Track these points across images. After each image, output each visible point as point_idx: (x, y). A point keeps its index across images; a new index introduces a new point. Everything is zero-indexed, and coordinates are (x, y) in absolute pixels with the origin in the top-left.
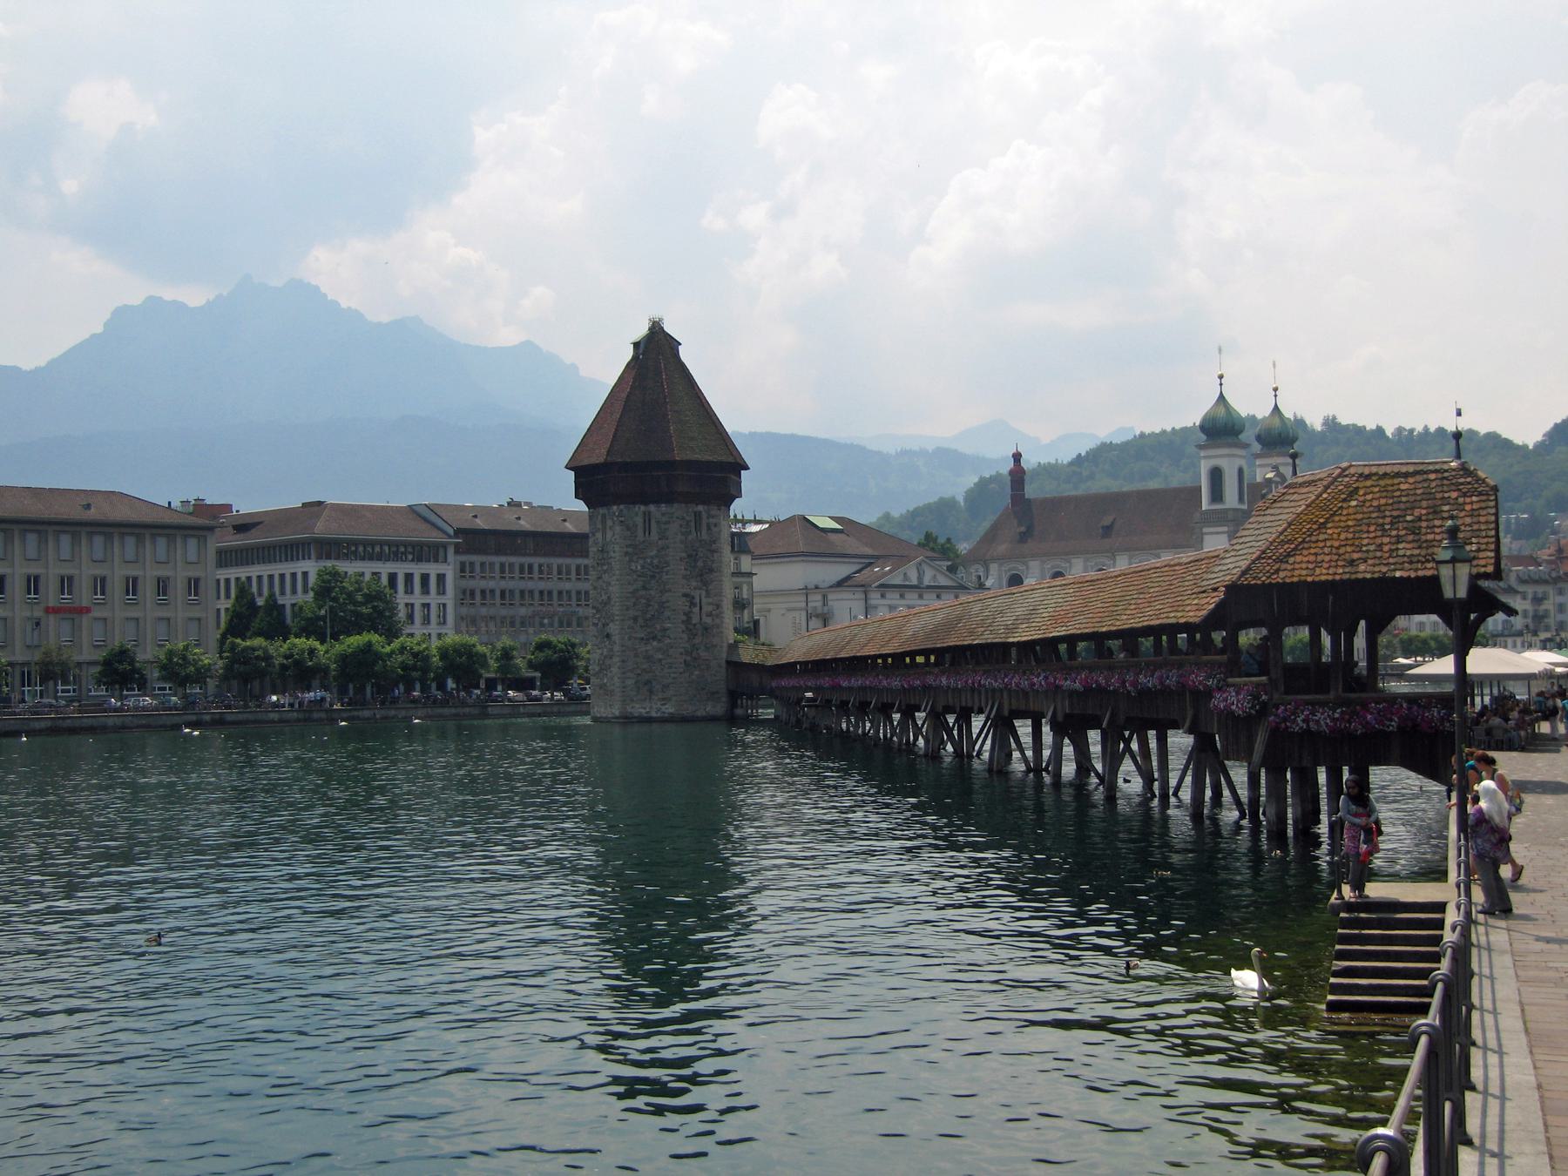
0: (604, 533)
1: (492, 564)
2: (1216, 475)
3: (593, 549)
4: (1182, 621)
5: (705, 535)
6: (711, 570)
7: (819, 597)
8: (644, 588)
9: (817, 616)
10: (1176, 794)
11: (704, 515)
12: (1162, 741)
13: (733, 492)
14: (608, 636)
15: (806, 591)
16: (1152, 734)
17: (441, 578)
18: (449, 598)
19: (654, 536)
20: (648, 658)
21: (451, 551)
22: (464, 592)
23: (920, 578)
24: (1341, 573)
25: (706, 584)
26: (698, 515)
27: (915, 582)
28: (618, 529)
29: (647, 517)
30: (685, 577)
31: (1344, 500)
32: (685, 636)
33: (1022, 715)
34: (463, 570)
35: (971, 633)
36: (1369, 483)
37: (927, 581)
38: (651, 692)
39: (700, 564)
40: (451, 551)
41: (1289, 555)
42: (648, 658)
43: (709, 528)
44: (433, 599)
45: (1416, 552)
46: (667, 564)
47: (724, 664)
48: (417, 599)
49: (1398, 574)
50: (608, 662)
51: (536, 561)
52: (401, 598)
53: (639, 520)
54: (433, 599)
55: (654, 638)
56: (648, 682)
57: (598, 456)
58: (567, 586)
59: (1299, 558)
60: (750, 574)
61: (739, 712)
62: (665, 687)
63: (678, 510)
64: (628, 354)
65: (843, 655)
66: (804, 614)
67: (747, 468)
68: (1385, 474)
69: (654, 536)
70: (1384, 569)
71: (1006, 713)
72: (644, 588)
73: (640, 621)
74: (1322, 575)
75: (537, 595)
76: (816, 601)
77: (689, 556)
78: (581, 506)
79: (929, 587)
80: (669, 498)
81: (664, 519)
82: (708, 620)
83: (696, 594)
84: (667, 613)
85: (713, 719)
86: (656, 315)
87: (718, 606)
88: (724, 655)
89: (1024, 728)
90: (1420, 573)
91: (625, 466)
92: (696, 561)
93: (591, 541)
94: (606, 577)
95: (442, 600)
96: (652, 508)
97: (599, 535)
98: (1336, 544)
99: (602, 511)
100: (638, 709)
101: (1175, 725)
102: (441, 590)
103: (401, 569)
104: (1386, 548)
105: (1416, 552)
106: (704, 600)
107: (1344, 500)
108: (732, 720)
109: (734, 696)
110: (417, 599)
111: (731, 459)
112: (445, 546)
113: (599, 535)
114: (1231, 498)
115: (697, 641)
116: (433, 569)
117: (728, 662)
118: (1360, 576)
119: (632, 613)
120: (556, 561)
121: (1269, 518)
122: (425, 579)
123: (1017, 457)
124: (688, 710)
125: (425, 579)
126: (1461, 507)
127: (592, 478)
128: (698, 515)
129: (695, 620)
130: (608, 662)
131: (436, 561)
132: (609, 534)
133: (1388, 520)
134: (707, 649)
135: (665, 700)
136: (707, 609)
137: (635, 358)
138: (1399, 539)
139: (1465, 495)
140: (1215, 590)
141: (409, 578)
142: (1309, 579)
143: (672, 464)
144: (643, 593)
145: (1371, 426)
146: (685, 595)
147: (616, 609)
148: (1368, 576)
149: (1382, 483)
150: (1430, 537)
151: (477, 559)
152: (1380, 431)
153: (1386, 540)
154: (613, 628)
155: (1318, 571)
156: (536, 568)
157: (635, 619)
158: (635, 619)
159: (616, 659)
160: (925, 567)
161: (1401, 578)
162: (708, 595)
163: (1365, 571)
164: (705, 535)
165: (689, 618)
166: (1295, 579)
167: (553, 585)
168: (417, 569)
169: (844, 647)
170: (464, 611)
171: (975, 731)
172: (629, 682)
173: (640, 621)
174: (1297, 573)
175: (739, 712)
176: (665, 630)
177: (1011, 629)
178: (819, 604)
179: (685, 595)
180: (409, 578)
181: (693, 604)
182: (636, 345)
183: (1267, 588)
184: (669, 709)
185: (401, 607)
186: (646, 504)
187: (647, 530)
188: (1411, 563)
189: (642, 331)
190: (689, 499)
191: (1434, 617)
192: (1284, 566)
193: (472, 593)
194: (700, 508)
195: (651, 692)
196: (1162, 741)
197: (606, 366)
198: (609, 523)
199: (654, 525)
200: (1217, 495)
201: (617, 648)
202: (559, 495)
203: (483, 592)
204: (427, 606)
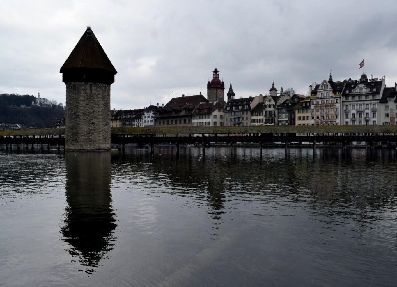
14: (93, 123)
20: (105, 131)
38: (105, 141)
42: (105, 131)
53: (104, 89)
55: (106, 125)
56: (105, 138)
69: (107, 94)
72: (105, 110)
73: (104, 119)
94: (92, 105)
99: (89, 83)
113: (88, 91)
127: (71, 72)
132: (94, 92)
144: (104, 111)
154: (94, 121)
157: (103, 119)
172: (102, 138)
173: (104, 119)
186: (105, 84)
195: (105, 141)
198: (94, 88)
201: (97, 127)
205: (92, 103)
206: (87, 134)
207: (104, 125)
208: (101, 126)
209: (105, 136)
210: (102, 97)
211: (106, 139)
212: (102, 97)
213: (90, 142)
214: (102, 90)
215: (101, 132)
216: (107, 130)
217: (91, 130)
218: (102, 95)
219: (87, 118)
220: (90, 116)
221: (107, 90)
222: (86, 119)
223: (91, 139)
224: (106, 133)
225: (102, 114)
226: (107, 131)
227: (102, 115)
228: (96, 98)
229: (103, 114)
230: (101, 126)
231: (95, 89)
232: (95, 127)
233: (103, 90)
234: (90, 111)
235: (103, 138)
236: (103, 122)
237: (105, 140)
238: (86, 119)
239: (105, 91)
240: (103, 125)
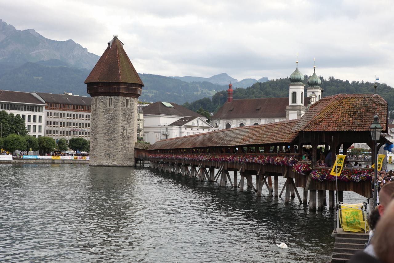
0: (96, 106)
1: (58, 114)
2: (294, 94)
3: (92, 110)
4: (285, 142)
5: (129, 107)
6: (131, 119)
7: (165, 129)
8: (108, 123)
9: (164, 135)
10: (280, 197)
11: (129, 101)
12: (276, 179)
13: (139, 94)
14: (96, 138)
15: (161, 127)
16: (273, 178)
17: (40, 117)
18: (43, 124)
19: (113, 106)
20: (109, 146)
21: (44, 108)
22: (47, 122)
23: (198, 124)
24: (337, 129)
25: (129, 122)
26: (127, 100)
27: (196, 125)
28: (101, 104)
29: (111, 100)
30: (122, 120)
31: (338, 106)
32: (122, 140)
33: (231, 170)
34: (48, 115)
35: (216, 142)
36: (346, 100)
37: (200, 125)
38: (109, 157)
39: (127, 116)
40: (44, 108)
41: (320, 122)
42: (109, 146)
43: (131, 105)
44: (37, 124)
45: (361, 123)
46: (117, 116)
47: (134, 149)
48: (32, 123)
49: (355, 130)
50: (96, 147)
51: (73, 113)
52: (27, 123)
53: (108, 101)
54: (37, 124)
55: (111, 140)
57: (96, 80)
58: (82, 121)
59: (323, 124)
60: (142, 120)
61: (138, 165)
62: (114, 156)
63: (121, 98)
64: (106, 46)
65: (173, 148)
66: (160, 133)
67: (143, 86)
68: (352, 98)
69: (113, 106)
70: (350, 128)
71: (226, 169)
72: (108, 123)
73: (107, 134)
74: (330, 129)
75: (72, 124)
76: (164, 130)
77: (124, 114)
78: (88, 96)
79: (200, 127)
80: (118, 94)
81: (116, 101)
82: (129, 135)
83: (126, 126)
84: (116, 132)
85: (130, 167)
86: (116, 34)
87: (133, 130)
88: (134, 146)
89: (231, 173)
90: (362, 130)
91: (104, 83)
92: (126, 115)
93: (91, 107)
94: (96, 119)
95: (40, 124)
96: (112, 97)
97: (94, 105)
98: (335, 120)
99: (96, 97)
100: (105, 163)
101: (281, 175)
102: (40, 121)
103: (27, 113)
104: (351, 122)
105: (361, 123)
106: (128, 128)
107: (338, 106)
108: (135, 167)
109: (136, 160)
110: (32, 123)
111: (139, 83)
112: (42, 106)
113: (94, 105)
114: (299, 102)
115: (125, 141)
116: (38, 114)
117: (135, 149)
118: (342, 130)
119: (104, 131)
120: (79, 113)
121: (313, 110)
122: (35, 117)
123: (230, 86)
124: (121, 163)
125: (35, 117)
126: (375, 109)
128: (127, 100)
129: (125, 134)
130: (96, 147)
131: (39, 111)
133: (352, 112)
134: (128, 144)
135: (114, 160)
136: (129, 131)
137: (108, 48)
138: (355, 118)
139: (377, 105)
140: (296, 132)
141: (29, 116)
142: (326, 130)
143: (119, 83)
144: (108, 125)
145: (344, 80)
146: (122, 126)
147: (99, 130)
148: (345, 130)
149: (351, 100)
150: (365, 118)
151: (53, 111)
152: (347, 82)
153: (351, 119)
154: (97, 136)
155: (329, 128)
156: (72, 116)
157: (105, 133)
158: (105, 133)
159: (98, 146)
160: (199, 120)
161: (356, 131)
162: (129, 126)
163: (344, 128)
164: (129, 107)
165: (123, 134)
166: (322, 130)
167: (78, 121)
168: (32, 114)
169: (174, 145)
170: (48, 128)
171: (215, 174)
173: (107, 134)
174: (322, 128)
175: (138, 165)
176: (115, 137)
177: (229, 142)
178: (165, 131)
179: (122, 126)
180: (29, 116)
181: (124, 129)
182: (109, 44)
183: (312, 133)
184: (115, 163)
185: (26, 126)
186: (110, 96)
187: (110, 104)
188: (359, 126)
189: (111, 39)
190: (125, 95)
191: (365, 144)
192: (318, 126)
193: (51, 122)
194: (128, 98)
196: (276, 179)
197: (98, 49)
198: (98, 102)
199: (112, 102)
200: (294, 101)
201: (98, 143)
202: (82, 92)
203: (54, 122)
204: (35, 126)
205: (96, 117)
206: (93, 150)
207: (107, 140)
208: (103, 141)
209: (108, 152)
210: (104, 111)
211: (111, 155)
212: (104, 111)
213: (94, 158)
214: (104, 103)
215: (101, 147)
216: (113, 146)
217: (95, 145)
218: (104, 108)
219: (93, 133)
220: (95, 131)
221: (114, 102)
222: (92, 135)
223: (94, 154)
224: (111, 149)
225: (104, 128)
226: (113, 147)
227: (103, 130)
228: (99, 112)
229: (105, 128)
230: (103, 141)
231: (98, 103)
232: (97, 143)
233: (106, 103)
234: (95, 126)
235: (105, 154)
236: (106, 137)
237: (108, 156)
238: (92, 135)
239: (110, 104)
240: (105, 140)
